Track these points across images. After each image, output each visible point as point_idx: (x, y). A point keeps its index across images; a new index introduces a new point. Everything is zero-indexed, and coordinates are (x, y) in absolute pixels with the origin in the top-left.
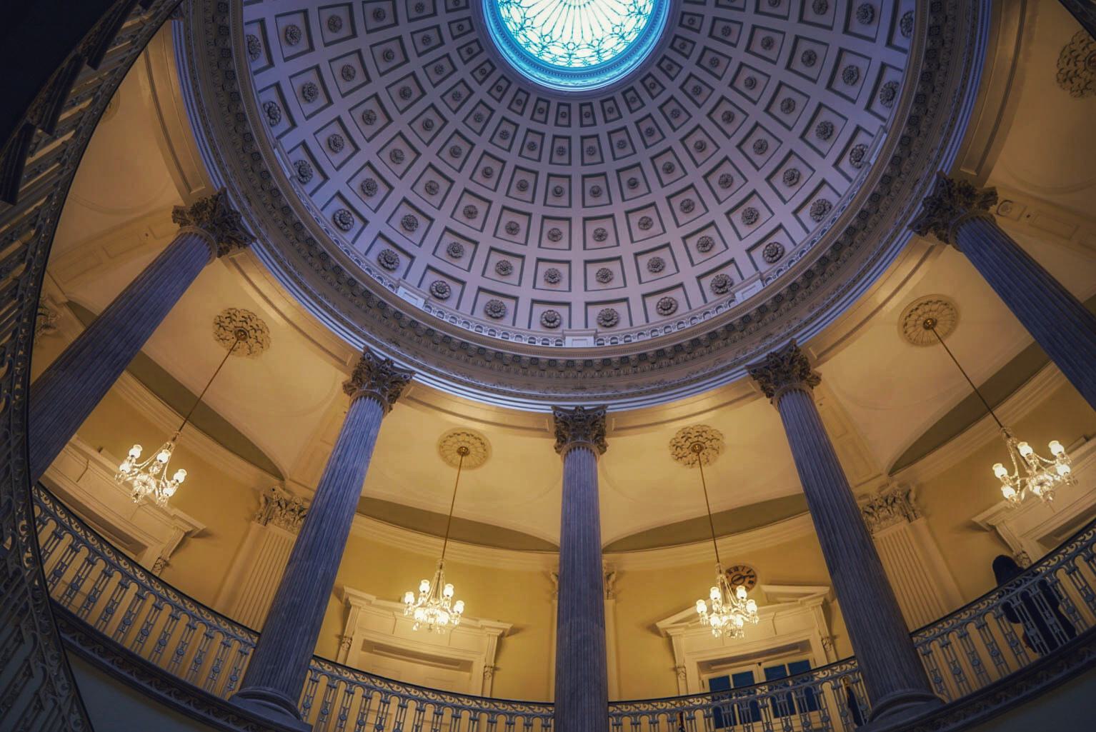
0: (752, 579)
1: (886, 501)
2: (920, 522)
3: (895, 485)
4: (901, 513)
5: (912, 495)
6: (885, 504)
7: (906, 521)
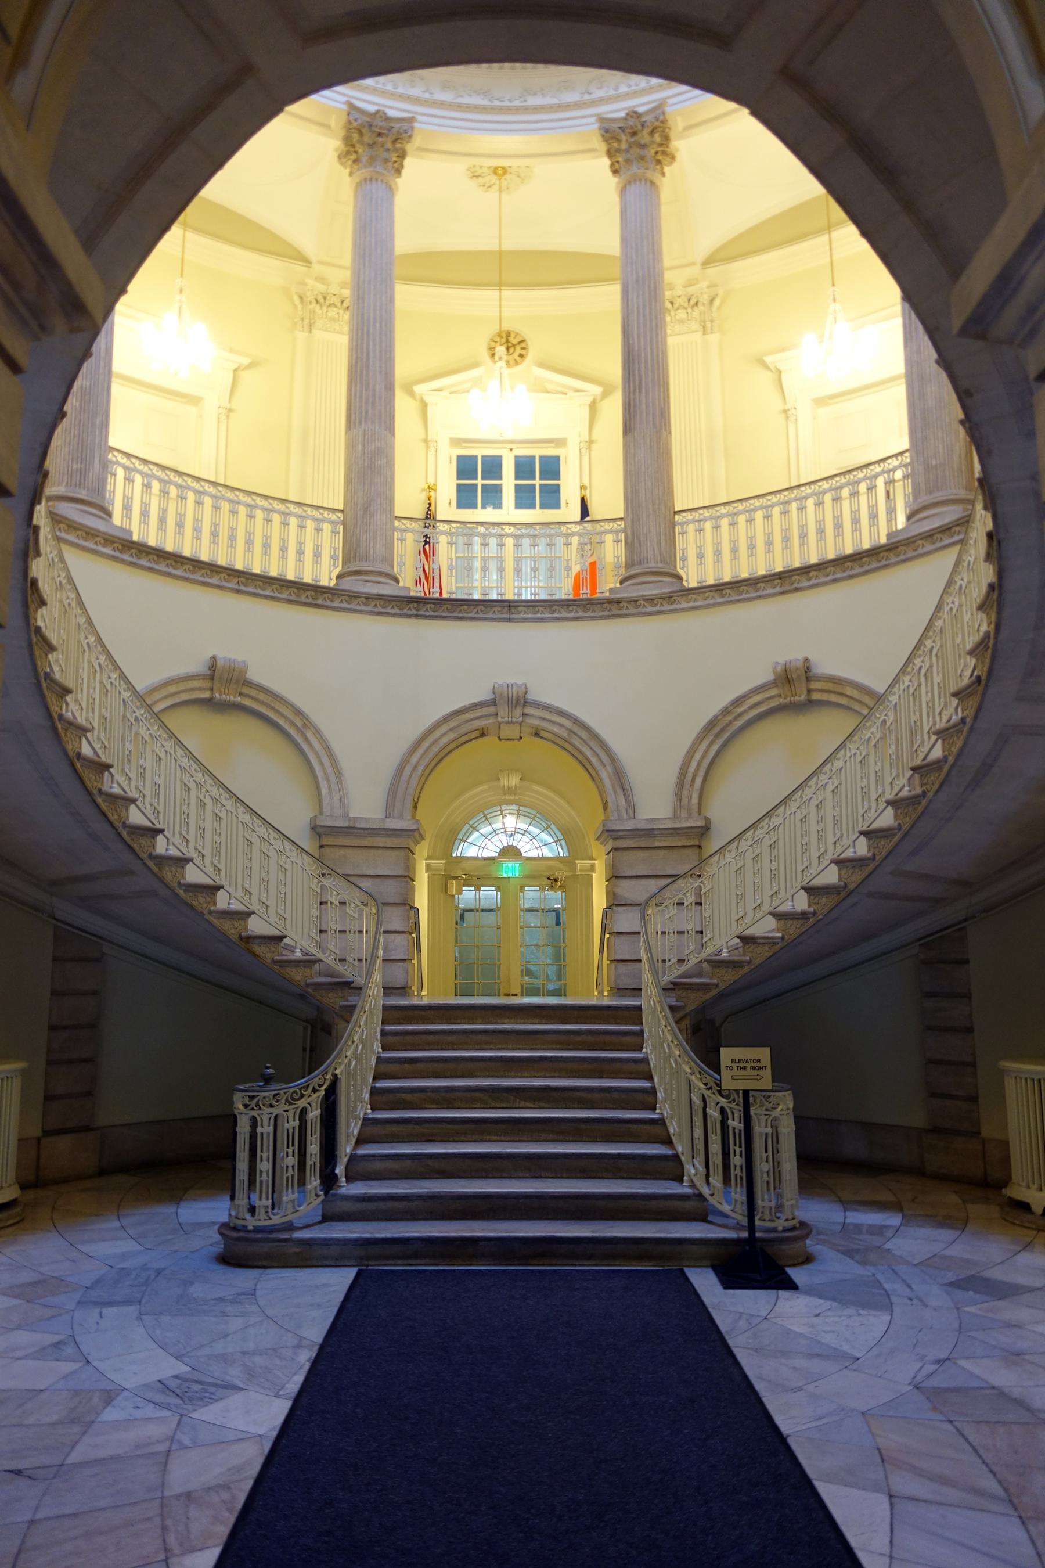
0: (523, 352)
1: (689, 300)
2: (714, 338)
3: (705, 284)
6: (686, 305)
7: (700, 334)
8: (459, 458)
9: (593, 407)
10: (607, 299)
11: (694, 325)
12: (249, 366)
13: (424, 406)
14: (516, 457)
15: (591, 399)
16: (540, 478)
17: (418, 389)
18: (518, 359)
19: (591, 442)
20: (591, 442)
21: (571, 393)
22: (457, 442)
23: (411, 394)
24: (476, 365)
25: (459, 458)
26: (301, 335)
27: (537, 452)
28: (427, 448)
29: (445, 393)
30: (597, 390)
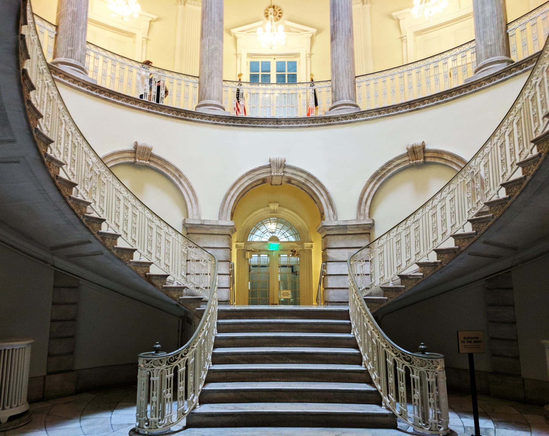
0: (280, 15)
2: (367, 6)
7: (361, 4)
9: (312, 38)
12: (157, 20)
13: (236, 39)
14: (277, 62)
17: (233, 31)
18: (278, 18)
19: (311, 54)
20: (311, 54)
21: (302, 32)
22: (250, 55)
23: (230, 33)
26: (180, 7)
27: (286, 60)
28: (237, 57)
30: (315, 30)
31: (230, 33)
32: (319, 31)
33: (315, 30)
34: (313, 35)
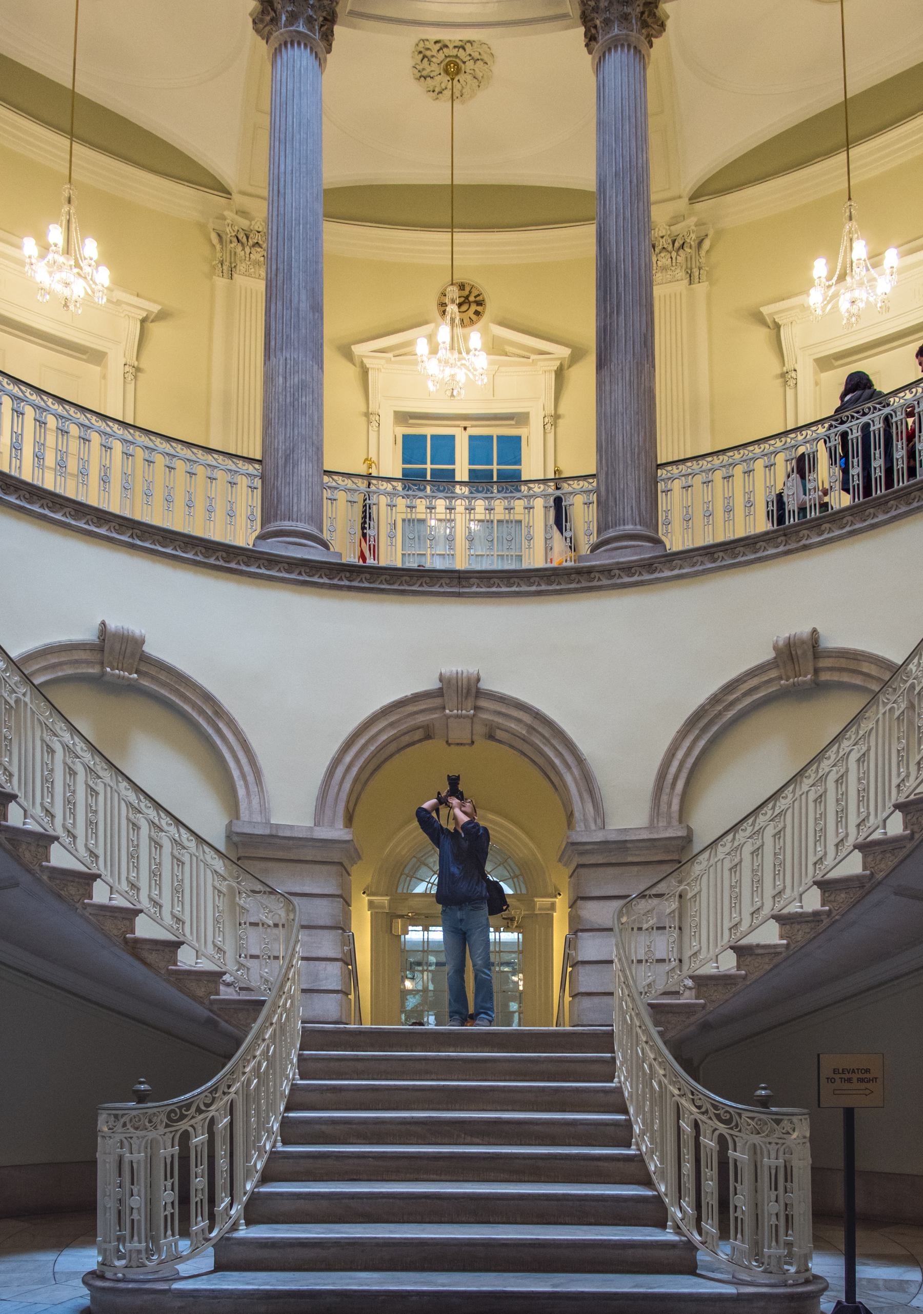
0: (479, 309)
1: (674, 242)
2: (701, 288)
3: (692, 221)
4: (684, 267)
5: (706, 244)
6: (670, 248)
7: (686, 281)
8: (406, 437)
9: (560, 374)
10: (578, 243)
11: (680, 274)
12: (162, 316)
14: (471, 438)
15: (558, 363)
16: (496, 470)
17: (358, 349)
18: (474, 317)
19: (556, 417)
20: (556, 417)
21: (533, 357)
22: (403, 417)
23: (347, 353)
24: (426, 323)
25: (406, 437)
26: (221, 282)
27: (495, 431)
28: (369, 422)
29: (390, 355)
30: (565, 352)
31: (347, 353)
32: (577, 356)
33: (565, 352)
34: (561, 365)
